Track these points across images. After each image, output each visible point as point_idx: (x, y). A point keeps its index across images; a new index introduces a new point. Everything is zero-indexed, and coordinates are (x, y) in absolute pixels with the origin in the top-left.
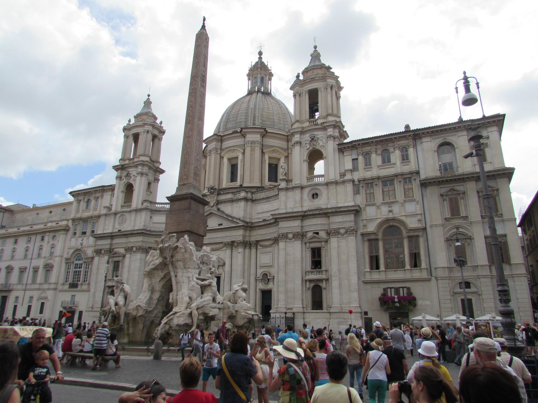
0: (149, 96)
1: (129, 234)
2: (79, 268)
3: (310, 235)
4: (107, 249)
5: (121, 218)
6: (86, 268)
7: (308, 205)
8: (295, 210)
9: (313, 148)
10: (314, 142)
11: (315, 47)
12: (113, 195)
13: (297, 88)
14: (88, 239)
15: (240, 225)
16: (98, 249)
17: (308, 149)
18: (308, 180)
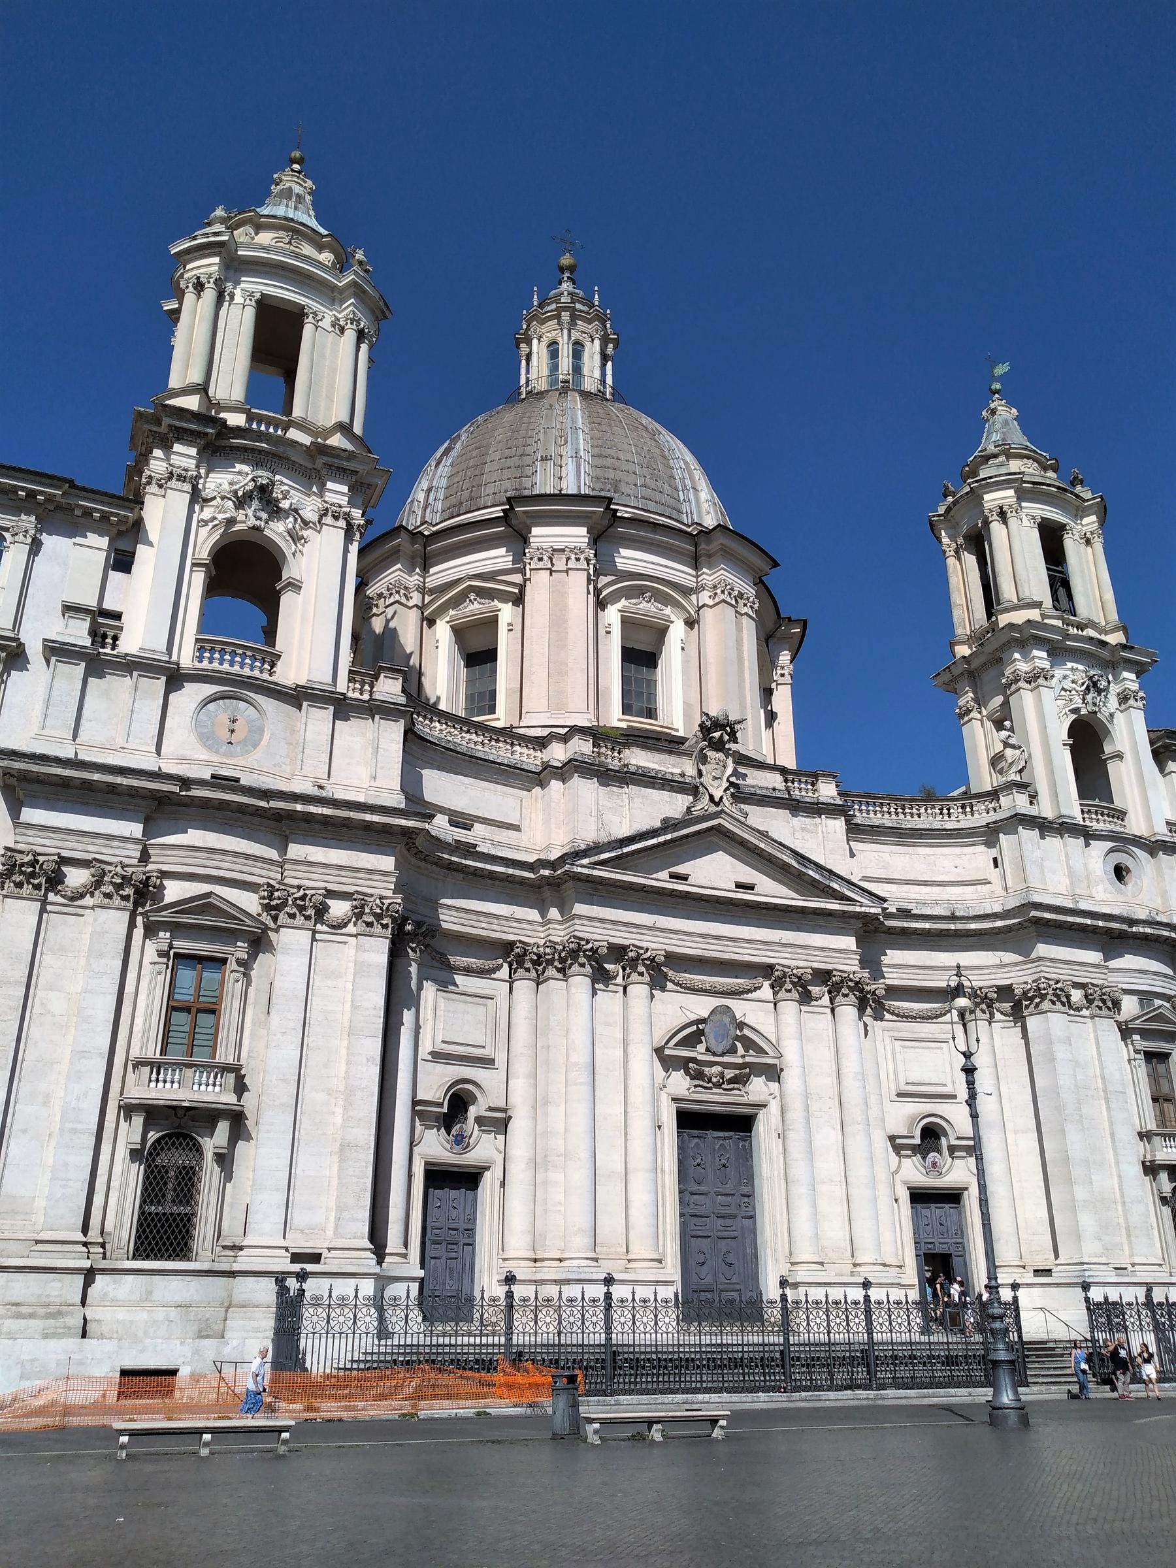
1: (308, 817)
3: (1130, 1007)
4: (124, 866)
5: (221, 712)
8: (1084, 905)
9: (1095, 713)
10: (1095, 695)
12: (122, 562)
13: (1011, 492)
15: (867, 910)
16: (36, 854)
17: (1075, 711)
18: (1082, 811)
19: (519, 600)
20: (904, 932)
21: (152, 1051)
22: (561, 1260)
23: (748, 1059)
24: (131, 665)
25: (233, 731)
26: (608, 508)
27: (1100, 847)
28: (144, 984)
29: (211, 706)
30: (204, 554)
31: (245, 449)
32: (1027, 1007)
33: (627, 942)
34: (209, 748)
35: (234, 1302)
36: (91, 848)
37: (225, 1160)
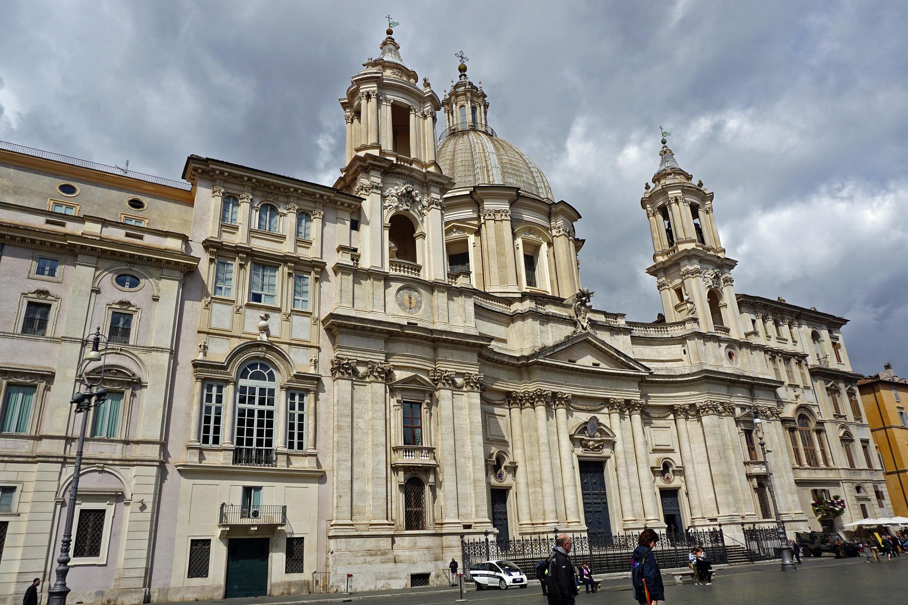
0: (389, 32)
1: (445, 341)
2: (262, 402)
3: (738, 411)
5: (405, 294)
6: (293, 408)
7: (727, 367)
8: (721, 370)
11: (664, 142)
14: (287, 320)
15: (644, 374)
19: (478, 233)
20: (652, 382)
21: (401, 443)
22: (544, 524)
23: (603, 438)
24: (369, 274)
25: (410, 303)
26: (517, 192)
27: (724, 345)
28: (392, 414)
29: (401, 292)
30: (387, 221)
31: (399, 173)
32: (702, 412)
33: (557, 391)
34: (403, 310)
35: (444, 546)
36: (367, 356)
37: (433, 489)
